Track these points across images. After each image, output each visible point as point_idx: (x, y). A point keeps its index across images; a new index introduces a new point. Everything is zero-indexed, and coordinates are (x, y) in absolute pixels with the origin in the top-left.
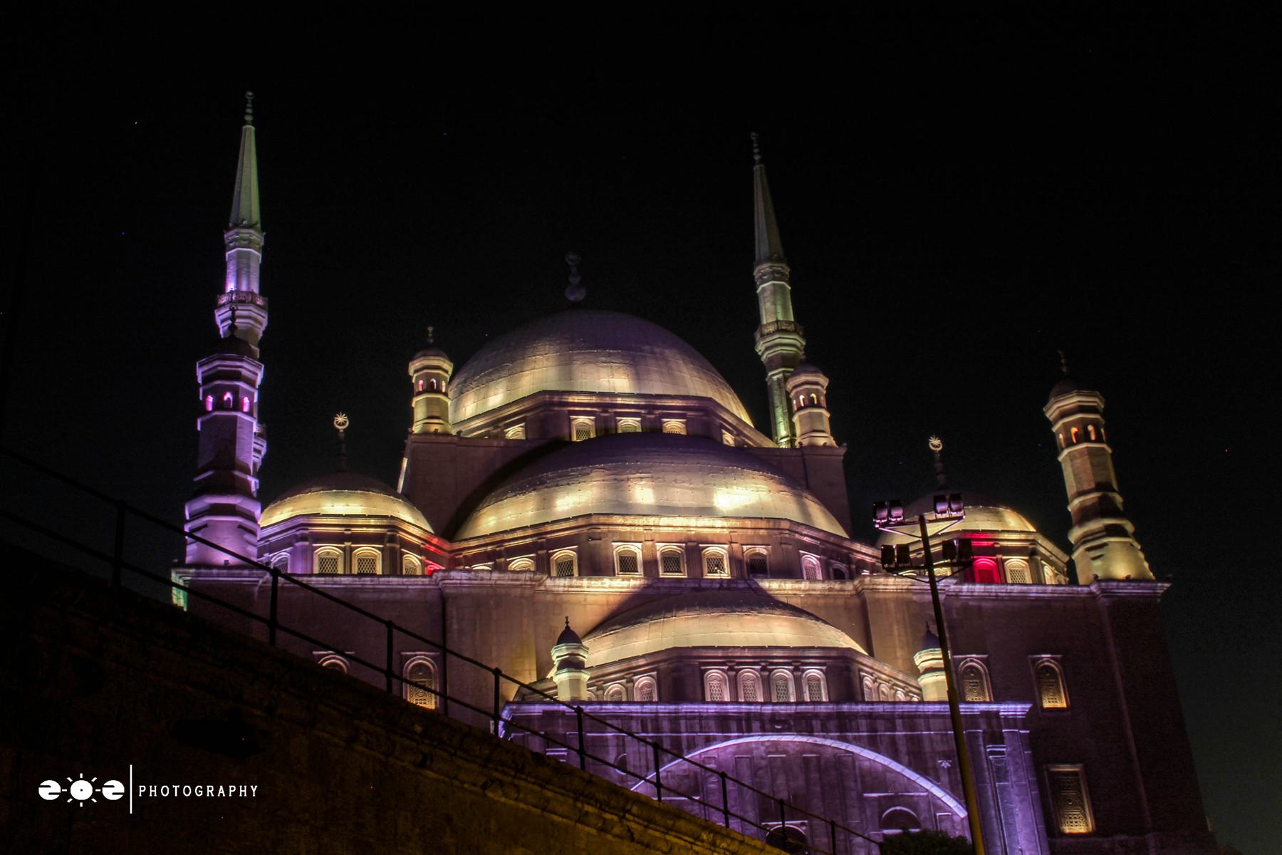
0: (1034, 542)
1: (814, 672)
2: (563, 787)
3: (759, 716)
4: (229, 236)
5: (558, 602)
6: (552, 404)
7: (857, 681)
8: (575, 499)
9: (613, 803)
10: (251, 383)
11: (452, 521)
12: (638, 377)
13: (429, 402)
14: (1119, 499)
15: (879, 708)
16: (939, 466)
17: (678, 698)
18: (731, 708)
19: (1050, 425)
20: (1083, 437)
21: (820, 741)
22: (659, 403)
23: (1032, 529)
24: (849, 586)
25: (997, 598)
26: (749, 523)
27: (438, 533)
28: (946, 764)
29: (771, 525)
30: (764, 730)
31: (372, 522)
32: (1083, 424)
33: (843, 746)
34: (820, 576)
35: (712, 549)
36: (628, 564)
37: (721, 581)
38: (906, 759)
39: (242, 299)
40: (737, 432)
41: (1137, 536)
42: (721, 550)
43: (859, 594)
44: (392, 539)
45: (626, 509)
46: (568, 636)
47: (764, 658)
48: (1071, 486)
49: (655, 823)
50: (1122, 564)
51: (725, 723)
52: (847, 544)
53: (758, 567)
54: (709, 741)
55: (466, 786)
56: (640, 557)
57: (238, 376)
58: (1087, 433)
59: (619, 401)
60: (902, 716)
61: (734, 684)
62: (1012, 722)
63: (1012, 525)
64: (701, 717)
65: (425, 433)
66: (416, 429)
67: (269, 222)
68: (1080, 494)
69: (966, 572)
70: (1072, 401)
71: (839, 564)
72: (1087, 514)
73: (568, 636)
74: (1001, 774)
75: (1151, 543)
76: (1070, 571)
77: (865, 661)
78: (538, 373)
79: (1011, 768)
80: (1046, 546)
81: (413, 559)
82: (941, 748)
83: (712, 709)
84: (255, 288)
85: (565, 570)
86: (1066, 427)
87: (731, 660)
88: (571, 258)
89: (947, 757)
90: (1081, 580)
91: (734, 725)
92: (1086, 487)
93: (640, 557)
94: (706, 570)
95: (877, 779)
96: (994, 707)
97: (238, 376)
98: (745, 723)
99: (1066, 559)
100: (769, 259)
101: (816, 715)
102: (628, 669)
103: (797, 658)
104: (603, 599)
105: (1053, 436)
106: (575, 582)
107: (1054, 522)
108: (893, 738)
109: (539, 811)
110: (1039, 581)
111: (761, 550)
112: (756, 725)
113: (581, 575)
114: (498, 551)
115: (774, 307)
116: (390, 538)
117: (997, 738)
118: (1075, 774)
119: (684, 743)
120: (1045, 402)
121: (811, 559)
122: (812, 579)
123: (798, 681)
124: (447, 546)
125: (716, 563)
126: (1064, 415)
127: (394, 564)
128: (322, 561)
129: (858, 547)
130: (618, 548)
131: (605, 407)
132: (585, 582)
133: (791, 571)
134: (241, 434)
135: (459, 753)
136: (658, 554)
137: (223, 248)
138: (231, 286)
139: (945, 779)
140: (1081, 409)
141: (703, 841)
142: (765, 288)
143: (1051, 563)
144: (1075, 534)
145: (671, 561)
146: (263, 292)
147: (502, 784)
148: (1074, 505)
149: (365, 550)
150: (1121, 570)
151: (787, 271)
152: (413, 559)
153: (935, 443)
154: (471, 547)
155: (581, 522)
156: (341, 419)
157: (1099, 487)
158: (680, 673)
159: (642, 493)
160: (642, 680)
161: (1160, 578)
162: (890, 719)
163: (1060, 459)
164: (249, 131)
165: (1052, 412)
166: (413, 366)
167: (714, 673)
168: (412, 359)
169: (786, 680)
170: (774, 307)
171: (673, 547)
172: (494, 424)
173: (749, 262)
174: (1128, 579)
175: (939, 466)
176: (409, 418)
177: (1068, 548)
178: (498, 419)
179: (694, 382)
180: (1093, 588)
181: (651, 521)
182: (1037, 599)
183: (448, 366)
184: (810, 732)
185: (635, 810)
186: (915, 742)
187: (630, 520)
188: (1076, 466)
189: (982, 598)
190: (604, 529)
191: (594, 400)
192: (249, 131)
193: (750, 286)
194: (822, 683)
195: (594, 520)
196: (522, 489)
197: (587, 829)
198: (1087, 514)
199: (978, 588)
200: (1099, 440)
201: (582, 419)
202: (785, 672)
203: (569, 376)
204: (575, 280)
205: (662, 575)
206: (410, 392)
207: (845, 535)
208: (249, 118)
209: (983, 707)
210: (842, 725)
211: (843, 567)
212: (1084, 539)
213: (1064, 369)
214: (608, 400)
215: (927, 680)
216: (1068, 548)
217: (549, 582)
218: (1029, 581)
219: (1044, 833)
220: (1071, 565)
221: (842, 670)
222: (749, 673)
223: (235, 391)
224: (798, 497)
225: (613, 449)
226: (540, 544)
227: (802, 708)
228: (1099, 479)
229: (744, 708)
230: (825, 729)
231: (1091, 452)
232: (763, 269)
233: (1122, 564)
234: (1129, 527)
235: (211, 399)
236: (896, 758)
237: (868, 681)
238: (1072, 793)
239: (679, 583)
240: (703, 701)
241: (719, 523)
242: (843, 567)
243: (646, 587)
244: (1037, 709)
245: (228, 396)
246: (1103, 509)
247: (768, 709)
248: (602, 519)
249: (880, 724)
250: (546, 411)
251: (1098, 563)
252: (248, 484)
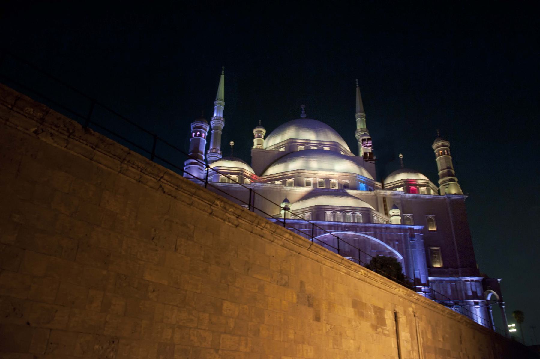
0: (428, 183)
1: (359, 214)
2: (109, 152)
3: (341, 226)
4: (215, 102)
5: (287, 193)
6: (293, 142)
7: (371, 218)
8: (295, 165)
9: (149, 169)
10: (206, 130)
11: (260, 172)
12: (317, 136)
13: (258, 140)
14: (453, 172)
15: (377, 225)
16: (402, 162)
17: (318, 219)
18: (332, 223)
19: (434, 150)
20: (443, 153)
21: (359, 234)
22: (323, 143)
23: (427, 179)
24: (373, 193)
25: (416, 198)
26: (344, 174)
27: (257, 173)
28: (397, 243)
29: (351, 175)
30: (342, 230)
31: (236, 169)
32: (443, 150)
33: (366, 236)
34: (365, 189)
35: (333, 181)
36: (308, 184)
37: (335, 190)
38: (385, 240)
39: (218, 119)
40: (344, 152)
41: (458, 182)
42: (336, 181)
43: (376, 195)
44: (242, 174)
45: (308, 169)
46: (286, 201)
47: (344, 210)
48: (439, 167)
49: (182, 188)
50: (454, 190)
51: (331, 227)
52: (373, 182)
53: (346, 187)
55: (19, 128)
56: (312, 183)
57: (201, 128)
58: (444, 153)
59: (312, 142)
60: (384, 228)
61: (334, 217)
62: (418, 231)
63: (422, 178)
64: (323, 225)
65: (256, 149)
66: (254, 147)
67: (226, 99)
68: (442, 170)
69: (408, 190)
70: (440, 143)
71: (370, 187)
72: (444, 176)
73: (286, 201)
74: (413, 246)
75: (462, 184)
76: (439, 192)
77: (375, 212)
78: (290, 134)
79: (417, 245)
80: (432, 185)
81: (247, 180)
82: (396, 238)
83: (327, 223)
84: (222, 116)
85: (290, 185)
86: (439, 151)
87: (334, 210)
88: (303, 107)
89: (397, 240)
90: (442, 194)
91: (333, 228)
92: (444, 168)
93: (312, 183)
94: (331, 186)
96: (412, 227)
97: (201, 128)
98: (337, 228)
99: (438, 189)
100: (360, 112)
101: (358, 227)
102: (304, 211)
103: (354, 210)
104: (301, 193)
105: (435, 154)
106: (292, 188)
107: (433, 177)
108: (381, 235)
109: (88, 160)
110: (429, 193)
111: (348, 182)
112: (340, 228)
113: (295, 186)
114: (272, 179)
115: (361, 125)
116: (241, 174)
117: (412, 236)
118: (437, 250)
119: (318, 233)
120: (432, 143)
121: (362, 185)
122: (362, 190)
123: (354, 217)
124: (258, 178)
125: (334, 185)
126: (438, 147)
127: (242, 180)
128: (222, 179)
129: (376, 183)
130: (306, 179)
131: (307, 143)
132: (295, 188)
133: (356, 188)
134: (201, 143)
135: (15, 109)
136: (317, 182)
137: (214, 105)
138: (215, 115)
139: (397, 247)
140: (443, 146)
141: (217, 205)
142: (358, 120)
143: (433, 190)
144: (440, 181)
145: (321, 184)
146: (223, 117)
147: (52, 135)
148: (440, 173)
149: (234, 177)
150: (453, 191)
151: (365, 115)
152: (247, 180)
153: (401, 156)
154: (265, 178)
155: (296, 172)
156: (232, 142)
157: (449, 168)
158: (319, 212)
159: (314, 163)
160: (307, 214)
161: (465, 194)
162: (381, 229)
163: (437, 160)
164: (223, 77)
165: (434, 147)
166: (255, 131)
167: (328, 214)
168: (254, 128)
169: (350, 216)
170: (361, 125)
171: (322, 180)
172: (277, 148)
173: (354, 112)
174: (455, 194)
175: (402, 162)
176: (253, 145)
177: (438, 185)
178: (278, 146)
179: (332, 137)
180: (445, 196)
181: (316, 172)
182: (428, 199)
183: (264, 131)
184: (356, 231)
185: (166, 177)
187: (310, 172)
188: (442, 161)
189: (412, 198)
190: (302, 174)
191: (304, 141)
192: (223, 77)
193: (355, 119)
194: (361, 218)
195: (299, 171)
196: (280, 163)
197: (128, 178)
198: (444, 176)
199: (411, 195)
200: (448, 154)
201: (301, 146)
202: (350, 214)
203: (298, 135)
204: (303, 112)
205: (318, 187)
206: (253, 137)
207: (373, 179)
208: (223, 73)
209: (409, 227)
210: (366, 230)
211: (372, 188)
212: (443, 182)
213: (438, 135)
214: (308, 142)
215: (393, 218)
216: (438, 185)
217: (285, 188)
218: (426, 193)
219: (426, 265)
220: (439, 191)
221: (367, 213)
222: (339, 214)
223: (200, 132)
225: (308, 152)
226: (284, 178)
227: (354, 224)
228: (448, 166)
229: (336, 223)
230: (361, 231)
231: (446, 158)
232: (357, 115)
233: (454, 190)
234: (456, 179)
235: (194, 134)
236: (382, 240)
237: (375, 218)
238: (436, 256)
239: (323, 189)
240: (325, 221)
241: (336, 173)
242: (372, 188)
243: (313, 190)
244: (425, 230)
245: (198, 133)
246: (449, 174)
247: (344, 224)
248: (302, 171)
249: (378, 230)
250: (291, 144)
251: (447, 189)
252: (202, 157)
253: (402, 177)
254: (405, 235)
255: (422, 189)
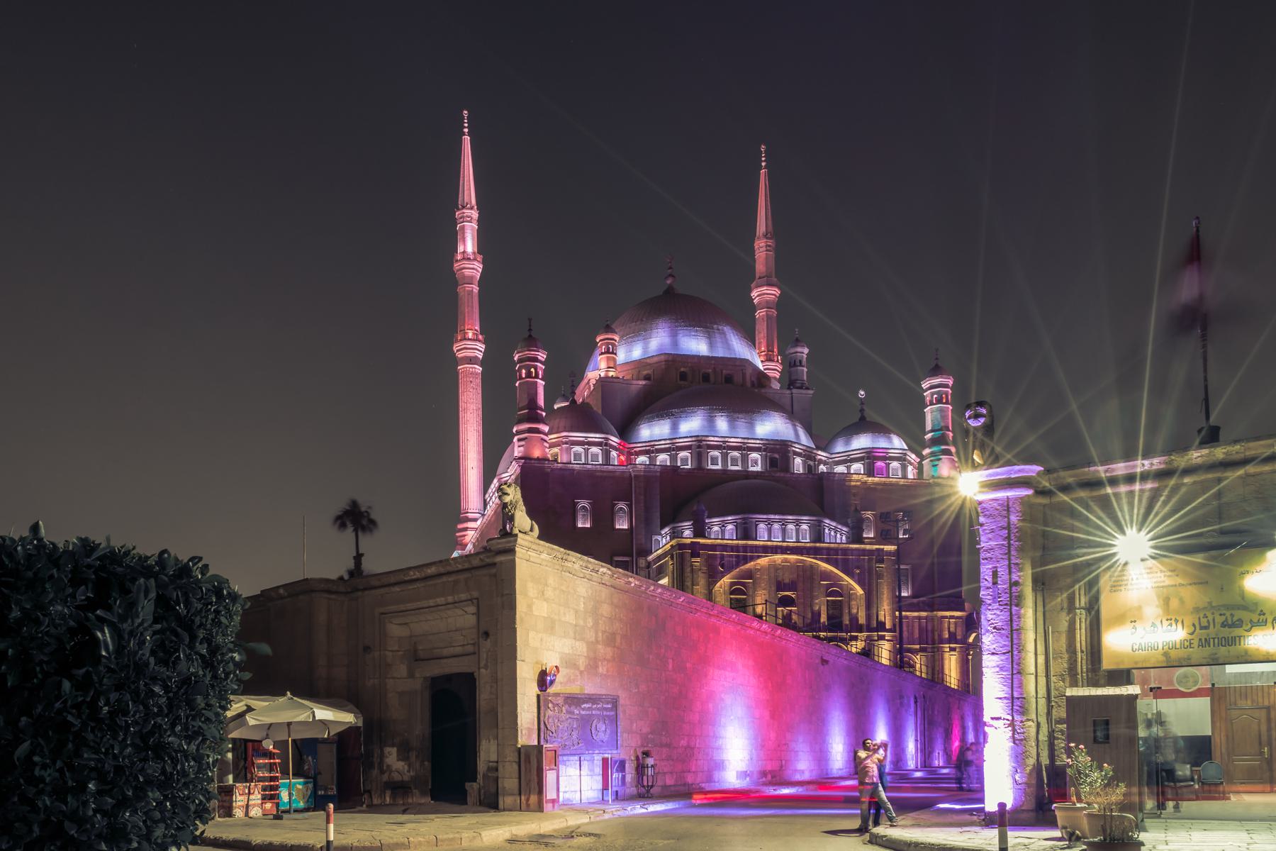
3: (781, 547)
25: (885, 484)
30: (782, 553)
44: (606, 444)
54: (759, 557)
62: (889, 553)
64: (756, 547)
69: (870, 472)
80: (912, 457)
95: (826, 575)
110: (905, 477)
117: (882, 561)
123: (797, 531)
149: (594, 450)
164: (467, 139)
186: (846, 561)
192: (467, 139)
224: (794, 426)
253: (862, 442)
254: (870, 560)
255: (895, 464)
